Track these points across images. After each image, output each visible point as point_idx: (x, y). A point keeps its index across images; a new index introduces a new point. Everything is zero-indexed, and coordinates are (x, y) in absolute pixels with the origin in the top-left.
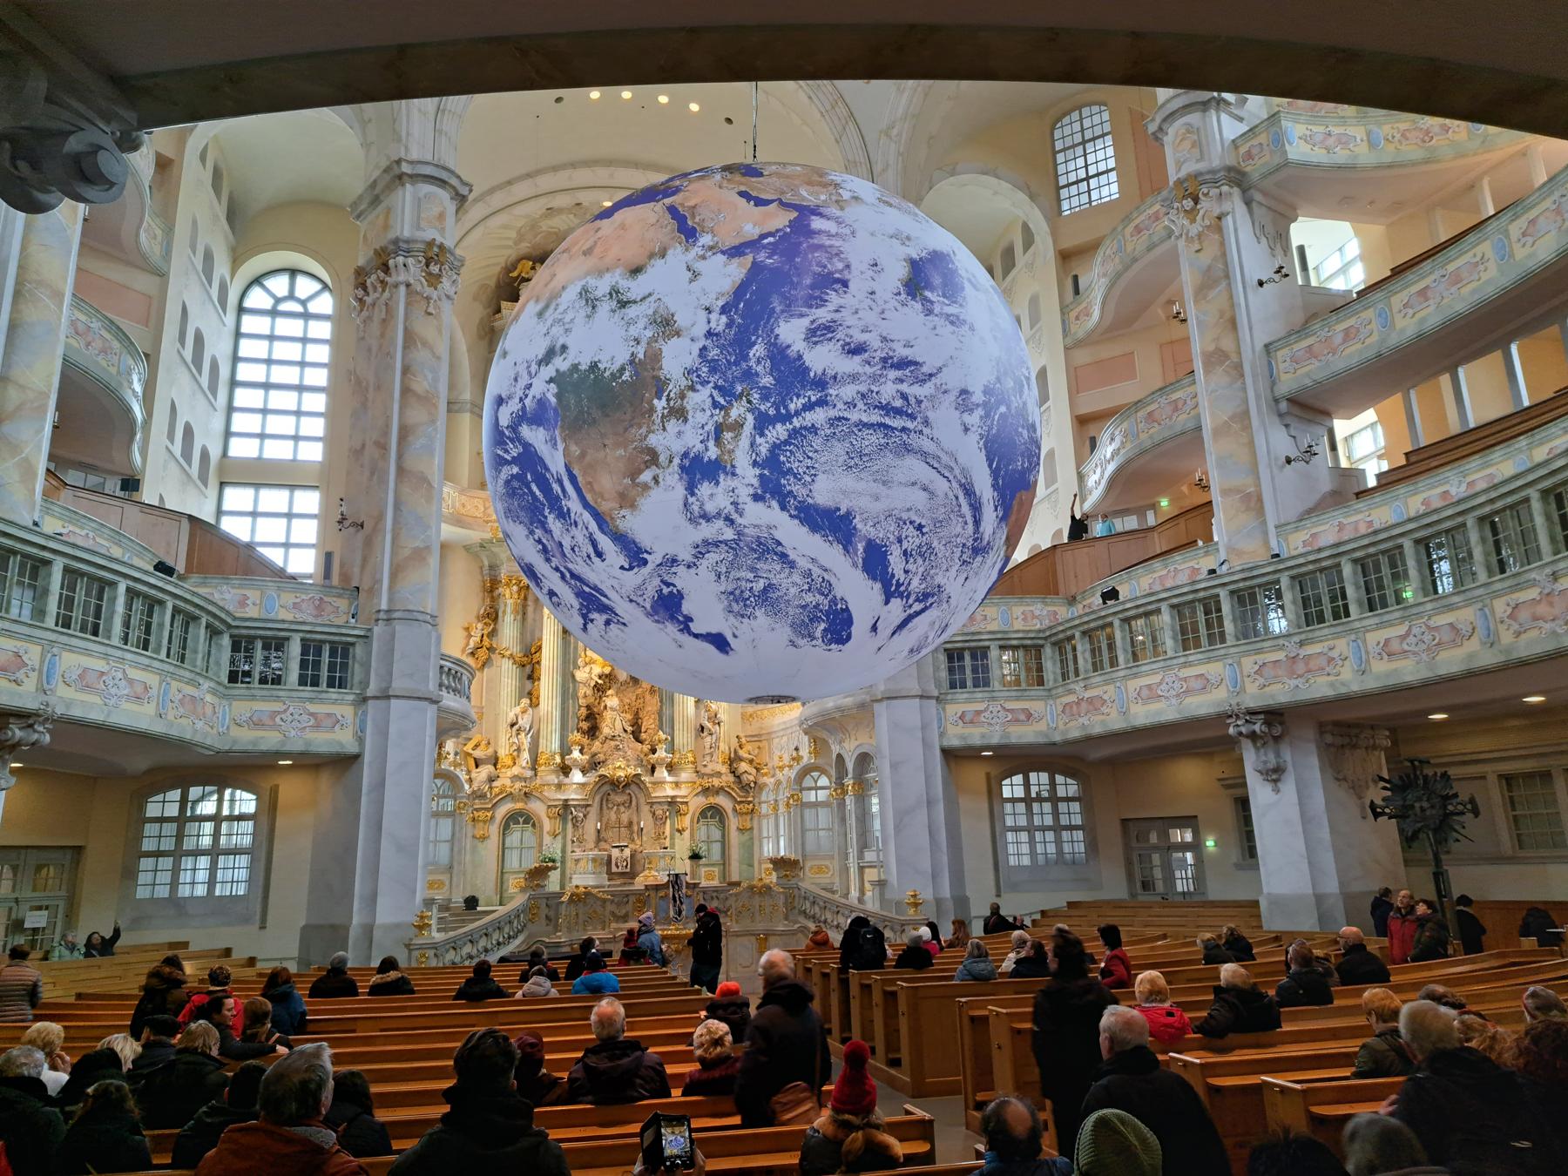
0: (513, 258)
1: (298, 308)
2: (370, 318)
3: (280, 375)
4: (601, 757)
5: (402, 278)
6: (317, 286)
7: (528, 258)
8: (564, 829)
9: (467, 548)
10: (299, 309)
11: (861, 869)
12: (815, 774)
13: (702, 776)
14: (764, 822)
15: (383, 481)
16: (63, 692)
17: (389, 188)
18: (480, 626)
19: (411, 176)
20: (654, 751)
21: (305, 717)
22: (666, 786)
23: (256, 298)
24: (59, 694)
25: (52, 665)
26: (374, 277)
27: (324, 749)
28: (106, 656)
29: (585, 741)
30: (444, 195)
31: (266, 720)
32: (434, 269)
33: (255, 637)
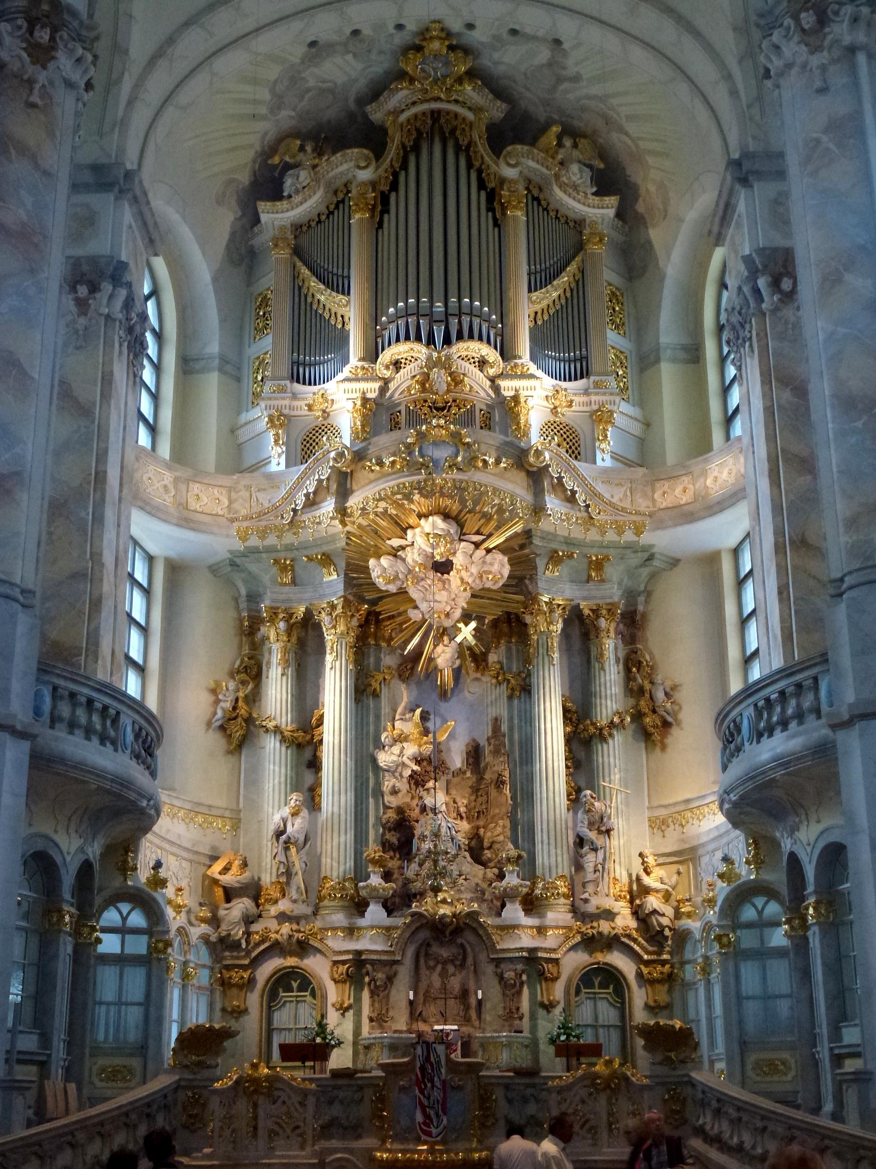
0: (272, 136)
9: (214, 569)
11: (838, 1060)
12: (760, 901)
18: (232, 685)
20: (501, 876)
22: (522, 932)
29: (394, 864)
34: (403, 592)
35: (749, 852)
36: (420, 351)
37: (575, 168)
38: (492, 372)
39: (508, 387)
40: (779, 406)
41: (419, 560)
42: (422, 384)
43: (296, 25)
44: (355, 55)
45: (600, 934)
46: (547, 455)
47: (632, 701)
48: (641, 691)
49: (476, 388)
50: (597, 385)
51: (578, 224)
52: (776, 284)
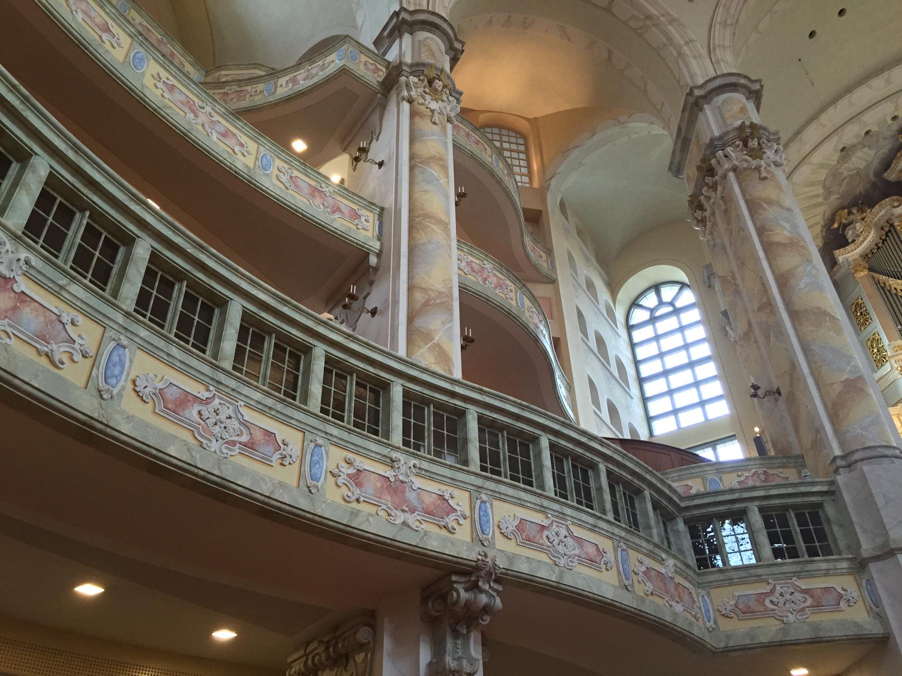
1: (670, 309)
2: (715, 225)
3: (672, 361)
5: (727, 166)
6: (676, 288)
7: (843, 208)
10: (670, 309)
15: (780, 333)
16: (501, 543)
21: (798, 596)
23: (639, 315)
24: (498, 546)
25: (484, 514)
28: (543, 510)
30: (738, 97)
31: (754, 605)
32: (753, 143)
43: (835, 139)
44: (869, 147)
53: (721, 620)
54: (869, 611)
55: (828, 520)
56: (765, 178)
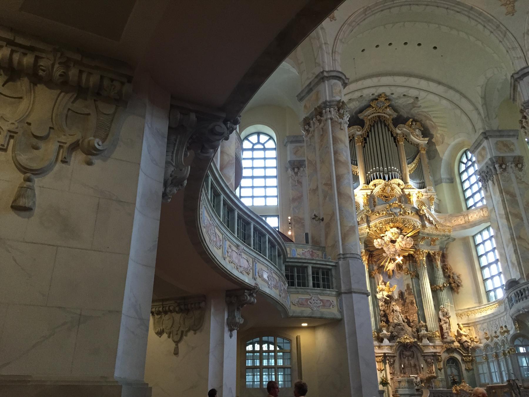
1: (262, 147)
2: (313, 136)
4: (396, 334)
6: (267, 138)
8: (385, 367)
10: (262, 147)
13: (445, 343)
14: (480, 367)
15: (332, 198)
17: (317, 84)
19: (327, 77)
21: (319, 301)
26: (314, 119)
27: (328, 316)
30: (339, 83)
33: (294, 266)
34: (382, 248)
35: (515, 325)
36: (382, 182)
37: (417, 130)
38: (402, 187)
39: (407, 191)
40: (507, 200)
41: (389, 240)
42: (383, 191)
45: (452, 348)
46: (425, 211)
47: (446, 279)
48: (449, 276)
49: (398, 192)
50: (429, 190)
51: (417, 145)
52: (501, 166)
53: (292, 306)
54: (338, 310)
55: (332, 275)
56: (342, 129)
